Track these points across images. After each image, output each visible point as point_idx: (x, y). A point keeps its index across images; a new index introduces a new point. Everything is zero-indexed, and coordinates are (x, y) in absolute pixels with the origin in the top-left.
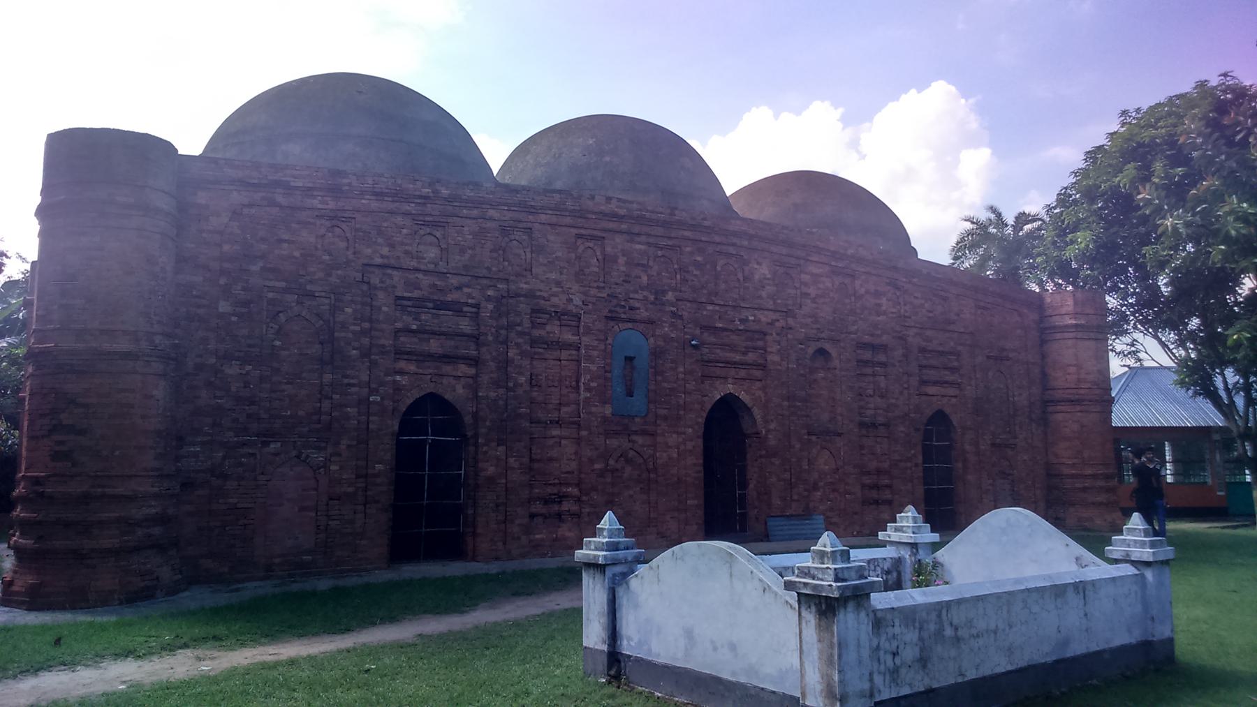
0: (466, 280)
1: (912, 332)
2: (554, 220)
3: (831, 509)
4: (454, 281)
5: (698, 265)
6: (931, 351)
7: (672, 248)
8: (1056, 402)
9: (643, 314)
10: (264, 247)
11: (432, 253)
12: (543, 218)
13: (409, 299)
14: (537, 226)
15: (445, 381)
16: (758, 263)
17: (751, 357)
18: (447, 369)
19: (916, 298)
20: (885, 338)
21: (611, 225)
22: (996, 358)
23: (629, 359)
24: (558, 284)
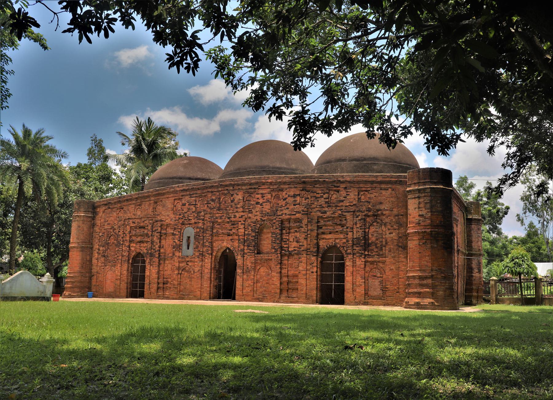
0: (145, 219)
1: (315, 210)
2: (168, 196)
3: (265, 291)
4: (143, 219)
5: (213, 200)
6: (326, 218)
7: (205, 196)
9: (193, 221)
10: (107, 219)
12: (165, 196)
16: (237, 195)
18: (142, 245)
19: (318, 194)
20: (298, 215)
21: (184, 193)
22: (374, 215)
24: (168, 216)
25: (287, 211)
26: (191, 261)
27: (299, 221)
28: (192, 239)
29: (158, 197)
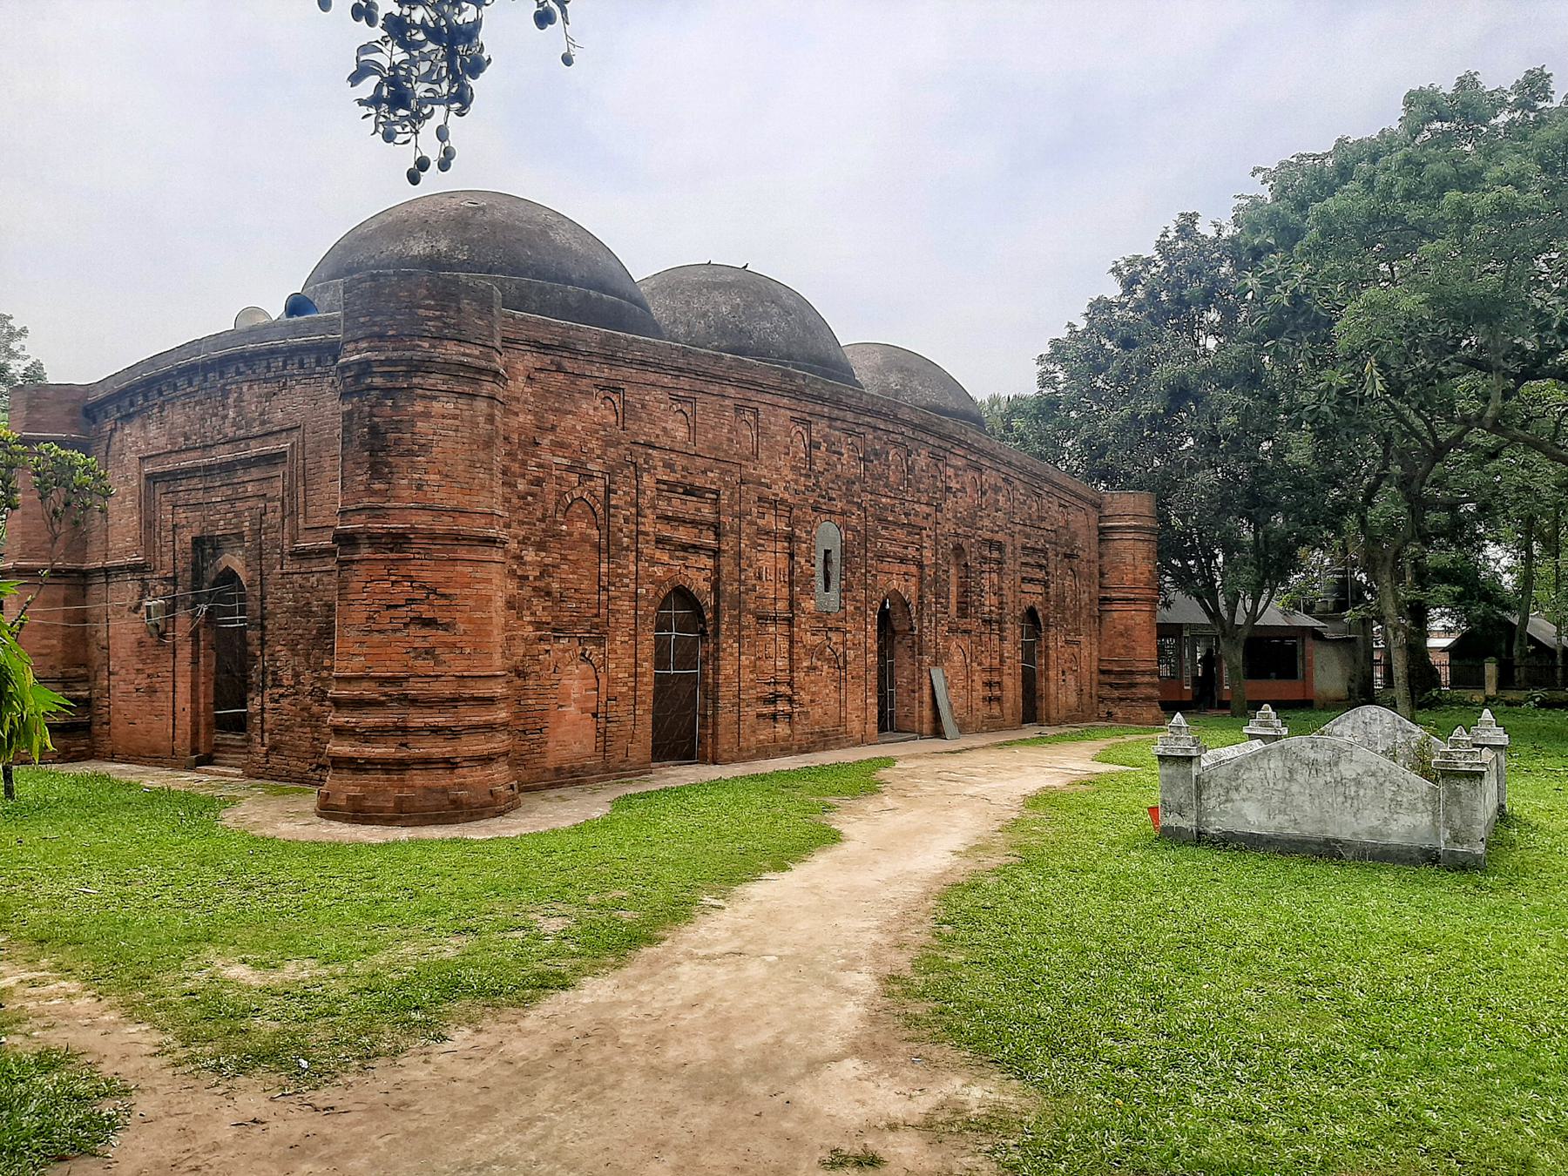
8: (1110, 600)
9: (839, 505)
11: (681, 433)
13: (664, 482)
14: (762, 408)
15: (689, 572)
17: (911, 552)
18: (692, 559)
23: (827, 552)
25: (986, 522)
26: (838, 629)
27: (1000, 547)
28: (836, 557)
29: (749, 394)
